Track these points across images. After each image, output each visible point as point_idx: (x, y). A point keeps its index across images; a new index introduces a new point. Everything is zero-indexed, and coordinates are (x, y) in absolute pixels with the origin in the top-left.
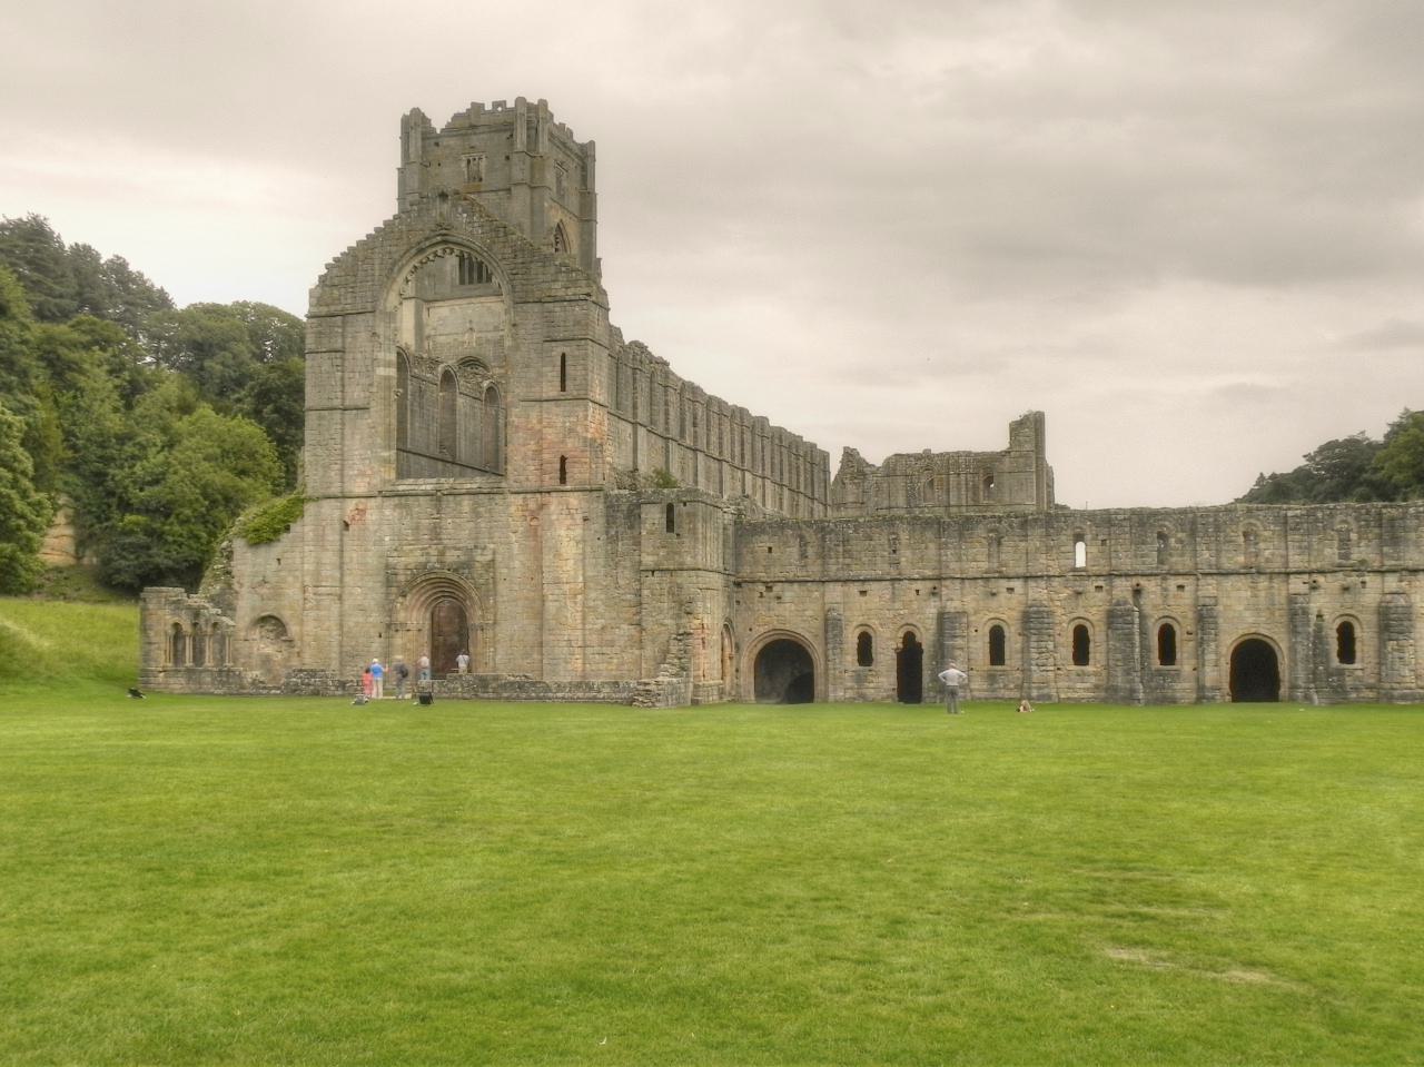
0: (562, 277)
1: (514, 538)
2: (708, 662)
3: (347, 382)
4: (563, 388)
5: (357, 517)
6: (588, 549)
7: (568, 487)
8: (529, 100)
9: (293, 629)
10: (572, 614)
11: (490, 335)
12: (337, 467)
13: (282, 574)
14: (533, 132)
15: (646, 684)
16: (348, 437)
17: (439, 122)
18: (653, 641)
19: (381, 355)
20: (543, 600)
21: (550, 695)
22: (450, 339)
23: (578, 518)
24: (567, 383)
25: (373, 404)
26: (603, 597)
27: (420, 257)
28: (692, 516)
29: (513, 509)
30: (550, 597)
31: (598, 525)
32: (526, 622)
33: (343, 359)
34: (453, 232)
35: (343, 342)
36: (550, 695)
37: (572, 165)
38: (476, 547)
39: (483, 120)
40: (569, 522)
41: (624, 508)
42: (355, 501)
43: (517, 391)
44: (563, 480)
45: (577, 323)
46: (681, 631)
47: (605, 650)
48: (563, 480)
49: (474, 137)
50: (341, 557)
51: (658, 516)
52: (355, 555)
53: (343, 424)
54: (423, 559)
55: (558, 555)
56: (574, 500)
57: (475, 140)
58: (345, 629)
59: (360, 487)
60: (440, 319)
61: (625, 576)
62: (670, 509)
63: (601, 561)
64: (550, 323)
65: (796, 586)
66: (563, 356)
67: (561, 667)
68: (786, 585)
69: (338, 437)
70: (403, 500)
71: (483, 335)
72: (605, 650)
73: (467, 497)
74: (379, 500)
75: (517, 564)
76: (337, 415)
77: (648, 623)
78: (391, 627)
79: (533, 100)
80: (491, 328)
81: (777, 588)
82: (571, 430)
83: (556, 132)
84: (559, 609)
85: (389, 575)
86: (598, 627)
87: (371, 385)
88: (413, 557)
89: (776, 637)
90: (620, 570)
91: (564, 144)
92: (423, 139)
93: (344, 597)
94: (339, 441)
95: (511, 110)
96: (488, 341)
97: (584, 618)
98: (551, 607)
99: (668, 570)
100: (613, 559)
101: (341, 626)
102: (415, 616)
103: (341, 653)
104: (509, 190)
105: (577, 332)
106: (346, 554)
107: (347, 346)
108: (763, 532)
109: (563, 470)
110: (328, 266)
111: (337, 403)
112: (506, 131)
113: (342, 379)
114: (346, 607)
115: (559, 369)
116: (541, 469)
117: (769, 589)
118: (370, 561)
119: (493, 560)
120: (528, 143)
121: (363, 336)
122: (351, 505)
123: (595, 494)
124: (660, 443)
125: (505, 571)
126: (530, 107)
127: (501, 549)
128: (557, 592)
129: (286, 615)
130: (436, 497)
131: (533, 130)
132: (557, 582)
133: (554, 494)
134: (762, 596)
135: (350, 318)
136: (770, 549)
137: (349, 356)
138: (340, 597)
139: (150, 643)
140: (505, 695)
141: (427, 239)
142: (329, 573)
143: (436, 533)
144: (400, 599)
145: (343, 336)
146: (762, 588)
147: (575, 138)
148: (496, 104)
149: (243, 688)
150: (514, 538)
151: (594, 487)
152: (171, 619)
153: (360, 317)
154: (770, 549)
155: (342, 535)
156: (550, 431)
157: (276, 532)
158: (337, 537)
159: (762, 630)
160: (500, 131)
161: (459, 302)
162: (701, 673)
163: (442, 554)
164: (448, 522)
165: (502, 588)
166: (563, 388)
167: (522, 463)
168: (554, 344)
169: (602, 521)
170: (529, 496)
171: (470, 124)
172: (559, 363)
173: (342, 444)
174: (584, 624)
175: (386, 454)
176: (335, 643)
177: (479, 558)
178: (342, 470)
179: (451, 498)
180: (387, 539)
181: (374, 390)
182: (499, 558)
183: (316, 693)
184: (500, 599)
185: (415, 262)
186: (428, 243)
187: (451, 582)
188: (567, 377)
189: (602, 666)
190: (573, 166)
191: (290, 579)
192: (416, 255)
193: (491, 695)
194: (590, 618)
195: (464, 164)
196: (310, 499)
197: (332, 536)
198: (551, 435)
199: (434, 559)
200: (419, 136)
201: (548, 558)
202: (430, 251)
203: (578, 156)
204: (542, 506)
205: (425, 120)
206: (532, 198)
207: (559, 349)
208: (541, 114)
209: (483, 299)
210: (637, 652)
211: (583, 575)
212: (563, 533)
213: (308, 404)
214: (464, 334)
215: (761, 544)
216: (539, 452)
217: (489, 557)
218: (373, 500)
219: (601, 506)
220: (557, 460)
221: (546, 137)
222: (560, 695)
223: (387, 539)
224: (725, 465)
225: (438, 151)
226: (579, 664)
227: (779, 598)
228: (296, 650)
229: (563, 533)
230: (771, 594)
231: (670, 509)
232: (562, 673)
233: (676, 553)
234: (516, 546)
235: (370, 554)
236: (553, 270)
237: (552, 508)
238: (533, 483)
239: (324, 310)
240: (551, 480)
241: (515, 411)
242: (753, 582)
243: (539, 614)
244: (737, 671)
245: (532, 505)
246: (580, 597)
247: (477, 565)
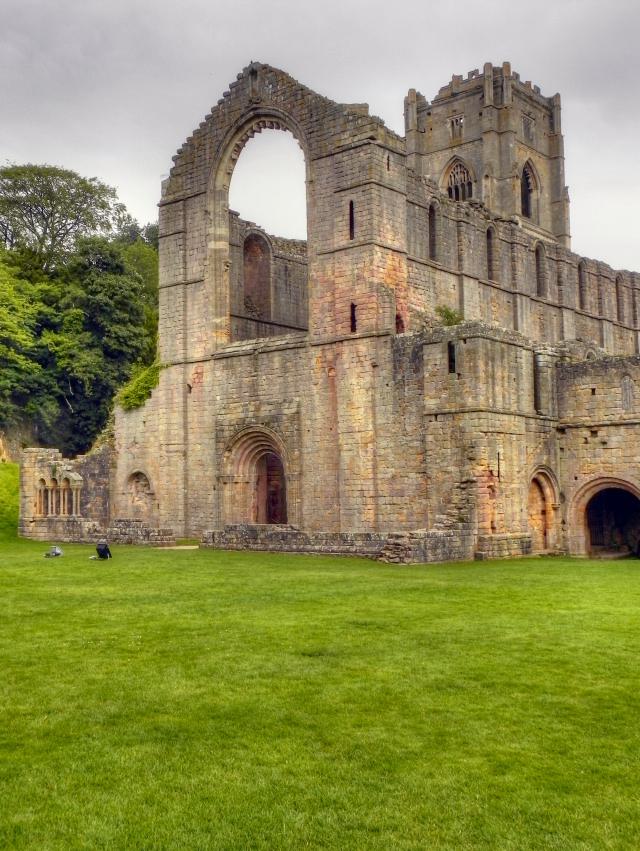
0: (350, 126)
1: (315, 389)
2: (511, 512)
3: (188, 257)
4: (352, 237)
5: (197, 380)
6: (378, 396)
7: (357, 335)
8: (495, 65)
9: (154, 483)
10: (364, 464)
12: (181, 336)
13: (147, 434)
14: (500, 89)
15: (398, 537)
16: (189, 308)
17: (430, 96)
18: (438, 491)
19: (211, 231)
20: (339, 449)
21: (309, 547)
23: (367, 364)
24: (356, 230)
25: (207, 276)
26: (392, 445)
27: (240, 135)
28: (472, 352)
29: (314, 361)
30: (345, 447)
31: (386, 371)
32: (327, 472)
33: (185, 239)
34: (263, 104)
35: (185, 224)
36: (309, 547)
37: (540, 115)
38: (285, 401)
39: (462, 88)
40: (358, 370)
41: (409, 351)
42: (195, 365)
43: (315, 245)
44: (353, 329)
45: (362, 168)
46: (464, 479)
47: (395, 500)
48: (353, 329)
49: (456, 103)
50: (185, 417)
51: (439, 356)
52: (196, 414)
53: (185, 297)
54: (242, 415)
55: (350, 404)
56: (363, 347)
57: (457, 105)
58: (190, 483)
59: (197, 353)
61: (411, 422)
62: (451, 348)
63: (390, 408)
64: (340, 174)
65: (622, 429)
66: (351, 204)
67: (355, 518)
68: (612, 429)
69: (181, 309)
70: (229, 360)
72: (395, 500)
73: (276, 353)
74: (212, 362)
75: (318, 415)
76: (180, 289)
77: (434, 472)
78: (221, 480)
79: (498, 63)
81: (602, 433)
82: (359, 277)
83: (521, 88)
84: (353, 459)
85: (218, 428)
86: (389, 476)
87: (205, 259)
88: (235, 415)
89: (604, 486)
90: (407, 416)
91: (531, 98)
92: (418, 112)
93: (189, 453)
94: (182, 313)
95: (482, 76)
97: (375, 467)
98: (346, 456)
99: (449, 413)
100: (400, 407)
101: (186, 479)
102: (244, 472)
103: (186, 504)
104: (481, 139)
105: (362, 178)
106: (189, 415)
107: (188, 227)
108: (585, 373)
109: (353, 319)
110: (175, 159)
111: (180, 278)
112: (479, 93)
113: (184, 256)
114: (190, 463)
115: (347, 217)
116: (335, 321)
117: (594, 433)
118: (206, 419)
119: (298, 413)
120: (495, 100)
121: (199, 215)
122: (192, 369)
123: (383, 339)
124: (504, 298)
125: (308, 422)
126: (496, 71)
127: (305, 401)
128: (350, 441)
129: (149, 471)
130: (253, 355)
131: (498, 87)
132: (350, 432)
133: (346, 343)
134: (586, 443)
135: (189, 202)
136: (593, 390)
137: (189, 236)
138: (185, 454)
139: (25, 497)
140: (271, 546)
141: (242, 116)
142: (176, 432)
143: (254, 387)
144: (227, 454)
145: (185, 219)
146: (586, 433)
147: (542, 93)
148: (471, 74)
149: (82, 537)
150: (315, 389)
151: (381, 332)
152: (38, 476)
153: (197, 199)
154: (593, 390)
155: (185, 397)
156: (341, 280)
157: (141, 398)
158: (182, 399)
159: (588, 478)
160: (474, 94)
162: (487, 524)
163: (258, 409)
164: (263, 379)
165: (307, 439)
166: (352, 237)
167: (322, 321)
168: (343, 194)
169: (389, 366)
170: (327, 347)
171: (452, 94)
172: (348, 212)
173: (185, 315)
174: (375, 473)
175: (218, 321)
176: (181, 496)
177: (286, 411)
178: (185, 338)
179: (265, 355)
180: (218, 398)
181: (207, 263)
182: (303, 410)
183: (129, 542)
184: (305, 451)
185: (236, 141)
186: (243, 120)
187: (264, 435)
188: (355, 224)
189: (394, 517)
190: (540, 115)
191: (152, 439)
192: (236, 133)
193: (260, 547)
194: (381, 468)
195: (449, 125)
196: (162, 367)
197: (178, 399)
198: (342, 284)
199: (251, 414)
200: (415, 110)
201: (342, 409)
202: (247, 128)
203: (546, 108)
204: (338, 355)
205: (419, 97)
206: (500, 142)
207: (348, 197)
208: (505, 74)
210: (424, 502)
211: (374, 423)
212: (354, 381)
213: (161, 283)
215: (584, 385)
216: (333, 303)
217: (294, 410)
218: (207, 363)
219: (389, 351)
220: (348, 308)
221: (510, 91)
222: (317, 547)
223: (218, 398)
224: (606, 325)
225: (430, 119)
226: (371, 515)
227: (604, 443)
228: (156, 502)
229: (354, 381)
230: (597, 440)
231: (451, 348)
232: (356, 524)
233: (456, 394)
234: (317, 398)
235: (206, 413)
236: (341, 121)
237: (345, 356)
238: (327, 336)
239: (171, 197)
240: (343, 330)
241: (314, 265)
242: (577, 427)
243: (336, 465)
244: (564, 522)
245: (330, 356)
246: (370, 445)
247: (285, 418)
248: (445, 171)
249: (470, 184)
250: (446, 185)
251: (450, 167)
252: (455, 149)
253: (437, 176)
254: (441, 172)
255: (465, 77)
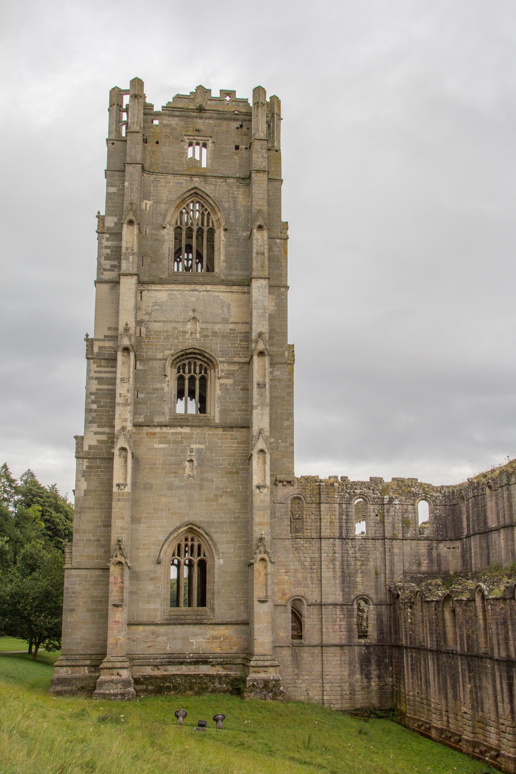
11: (217, 327)
22: (169, 327)
49: (200, 121)
60: (155, 304)
71: (209, 326)
80: (219, 319)
92: (145, 114)
96: (215, 334)
148: (225, 93)
161: (181, 287)
171: (195, 109)
209: (209, 287)
214: (185, 323)
248: (178, 202)
249: (211, 232)
250: (174, 222)
251: (183, 201)
252: (196, 179)
253: (163, 207)
254: (169, 202)
255: (215, 94)
